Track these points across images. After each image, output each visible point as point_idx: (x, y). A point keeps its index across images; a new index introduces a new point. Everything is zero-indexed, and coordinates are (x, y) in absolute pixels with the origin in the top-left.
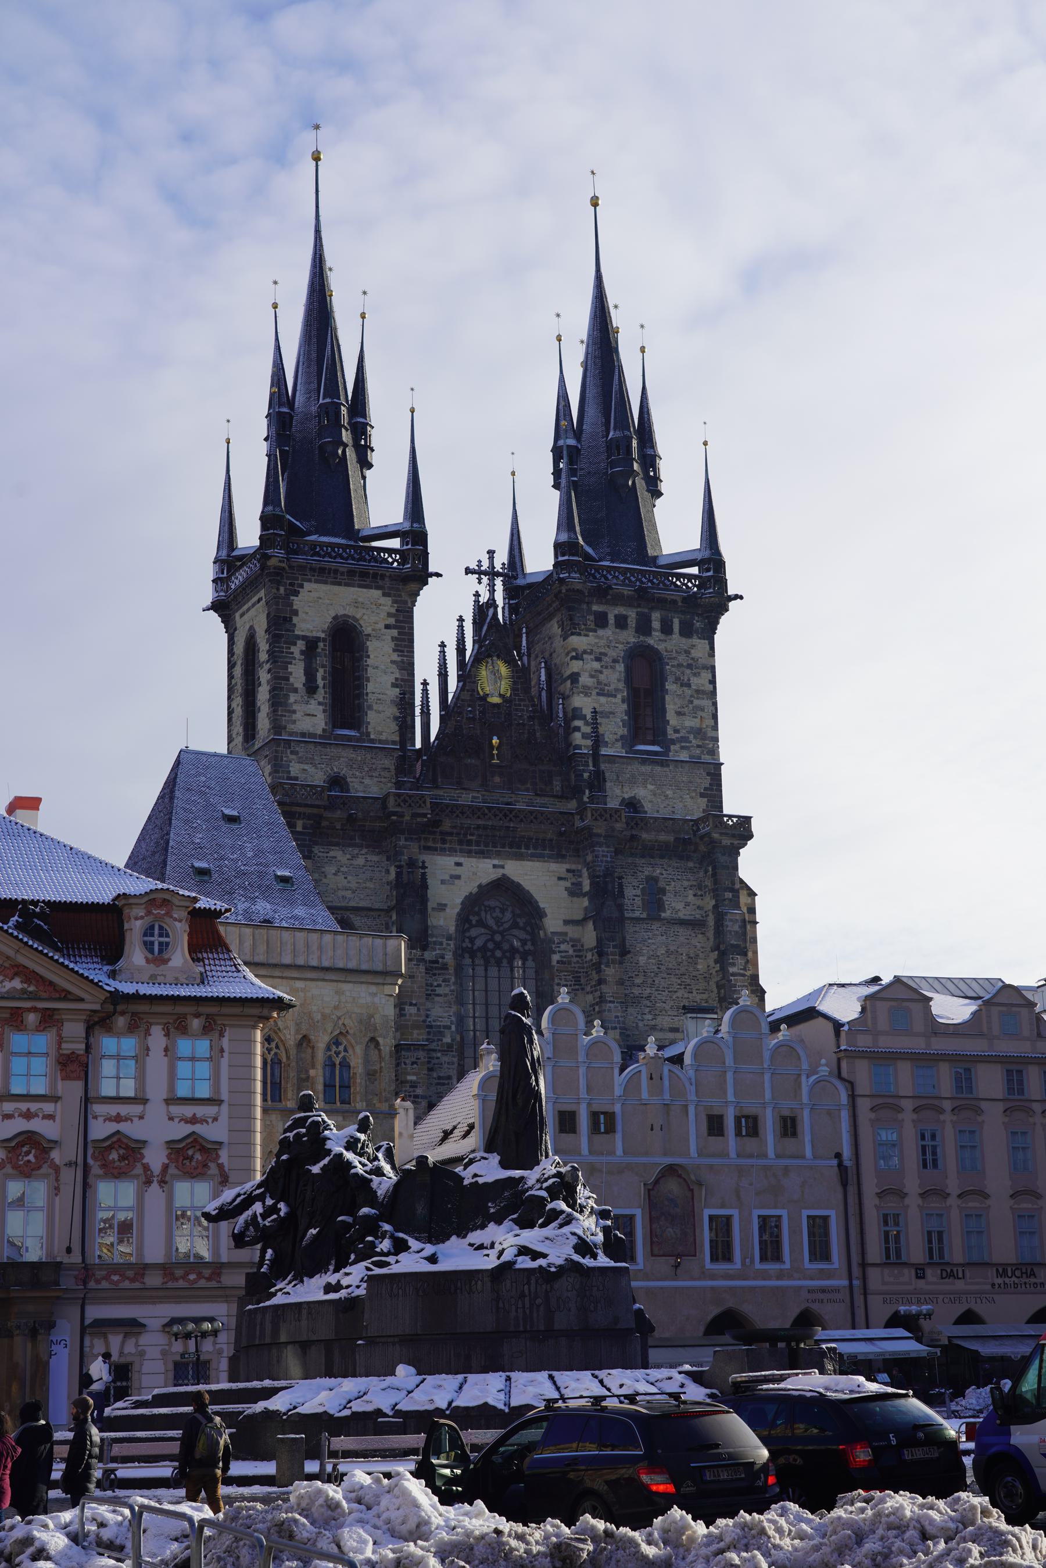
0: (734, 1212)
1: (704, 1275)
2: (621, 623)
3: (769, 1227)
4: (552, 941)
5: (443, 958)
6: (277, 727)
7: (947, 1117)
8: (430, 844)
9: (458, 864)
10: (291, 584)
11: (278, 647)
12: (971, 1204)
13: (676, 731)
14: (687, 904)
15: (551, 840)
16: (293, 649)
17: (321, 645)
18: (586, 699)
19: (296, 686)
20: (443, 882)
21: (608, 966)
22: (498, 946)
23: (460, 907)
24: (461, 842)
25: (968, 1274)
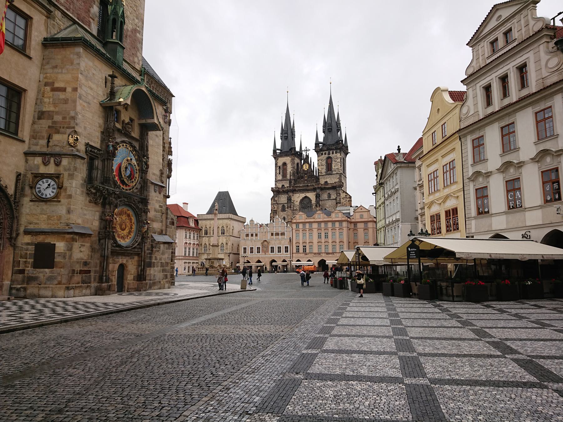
1: (270, 255)
2: (325, 154)
6: (276, 179)
7: (307, 231)
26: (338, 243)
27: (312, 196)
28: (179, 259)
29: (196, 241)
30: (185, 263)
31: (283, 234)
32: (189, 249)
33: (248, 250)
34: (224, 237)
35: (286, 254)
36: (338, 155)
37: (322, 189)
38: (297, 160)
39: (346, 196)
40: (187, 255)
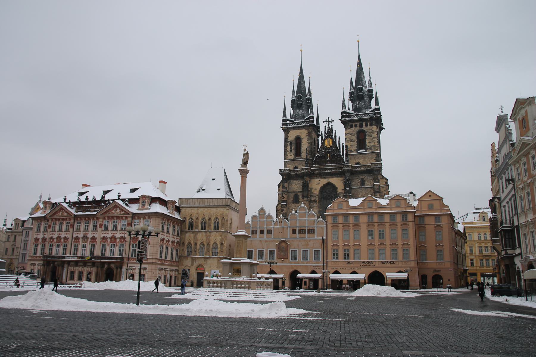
0: (297, 250)
1: (289, 262)
2: (356, 126)
3: (305, 252)
4: (339, 194)
6: (285, 159)
8: (314, 177)
9: (319, 180)
12: (356, 247)
13: (369, 146)
15: (339, 173)
16: (288, 144)
17: (293, 142)
18: (348, 144)
20: (316, 184)
22: (329, 196)
24: (320, 176)
25: (354, 263)
26: (400, 246)
27: (338, 182)
28: (152, 263)
29: (176, 237)
30: (160, 270)
31: (311, 231)
32: (167, 248)
33: (255, 254)
34: (218, 234)
35: (317, 263)
36: (375, 128)
37: (352, 173)
38: (314, 135)
40: (164, 258)
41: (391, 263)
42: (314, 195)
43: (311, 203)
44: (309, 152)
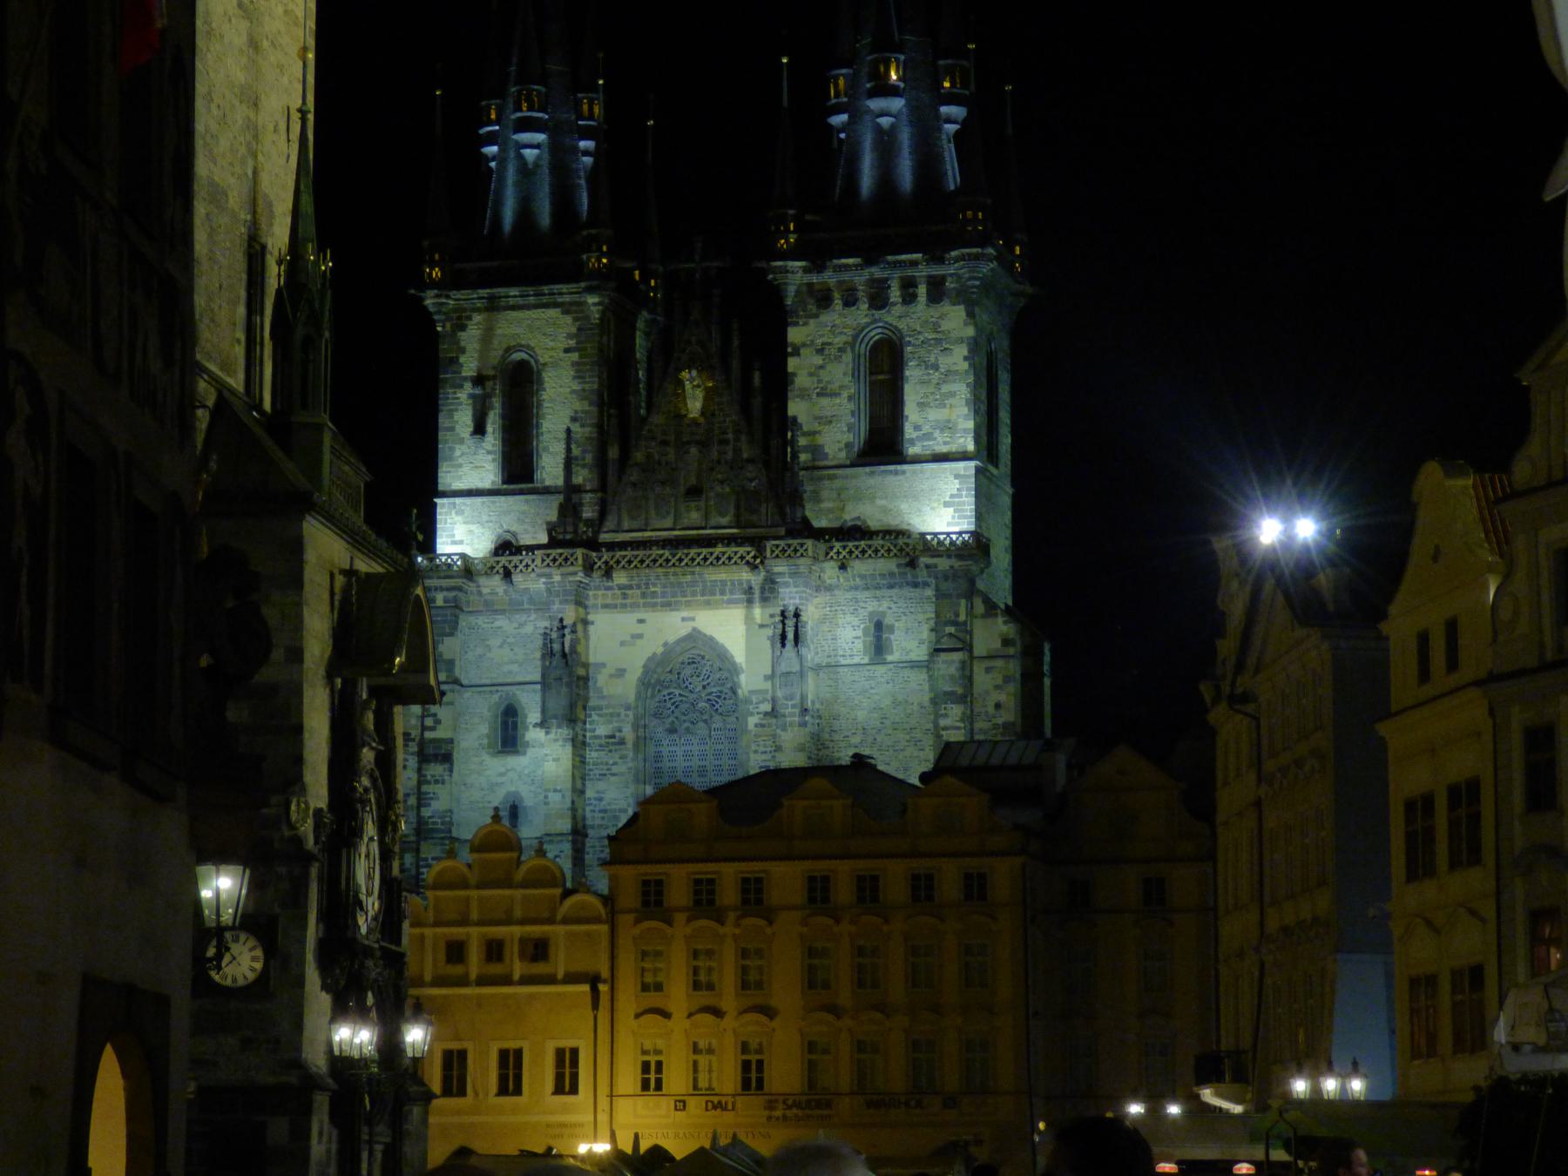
0: (468, 1046)
2: (850, 301)
4: (747, 701)
5: (620, 731)
8: (609, 601)
9: (641, 621)
10: (459, 318)
11: (444, 394)
13: (917, 428)
14: (921, 642)
19: (463, 435)
20: (623, 644)
21: (784, 729)
23: (641, 670)
24: (644, 595)
25: (739, 1105)
39: (1006, 642)
41: (907, 1104)
42: (608, 707)
43: (594, 754)
44: (584, 452)
